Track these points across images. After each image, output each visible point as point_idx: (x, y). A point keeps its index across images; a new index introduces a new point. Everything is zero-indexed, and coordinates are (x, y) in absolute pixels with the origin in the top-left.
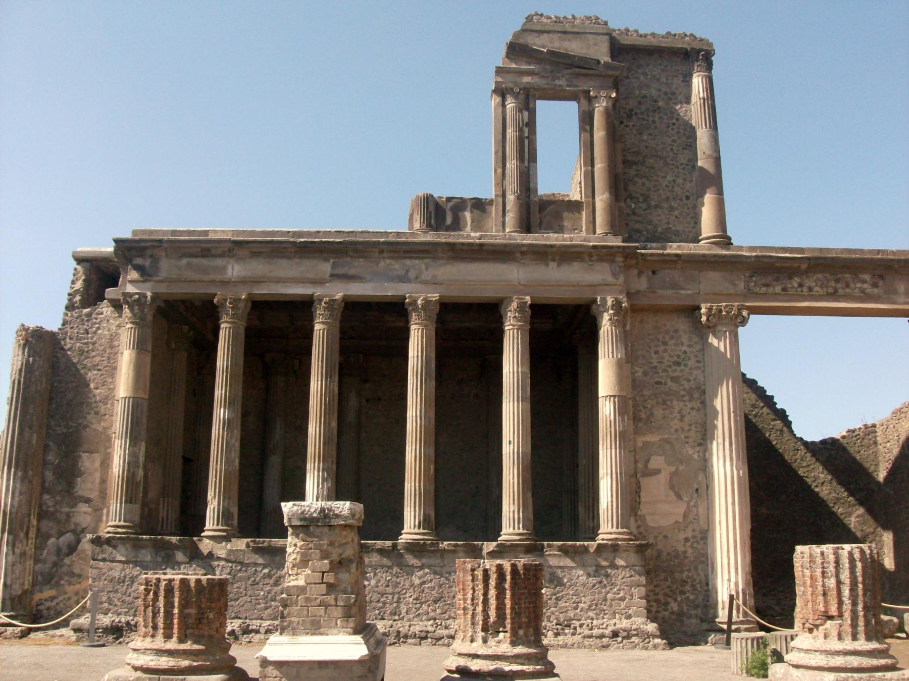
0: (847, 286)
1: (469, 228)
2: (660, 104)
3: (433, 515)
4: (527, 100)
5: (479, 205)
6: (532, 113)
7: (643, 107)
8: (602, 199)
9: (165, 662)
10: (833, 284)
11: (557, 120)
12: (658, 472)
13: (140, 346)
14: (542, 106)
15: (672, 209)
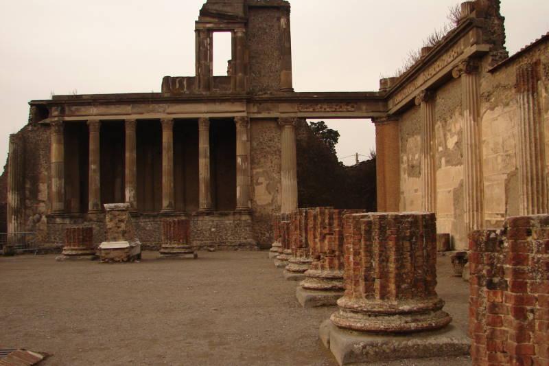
0: (341, 107)
1: (185, 90)
2: (267, 31)
3: (173, 202)
5: (189, 79)
6: (211, 39)
7: (260, 32)
9: (74, 253)
10: (334, 107)
12: (262, 183)
13: (59, 142)
14: (216, 35)
15: (270, 76)
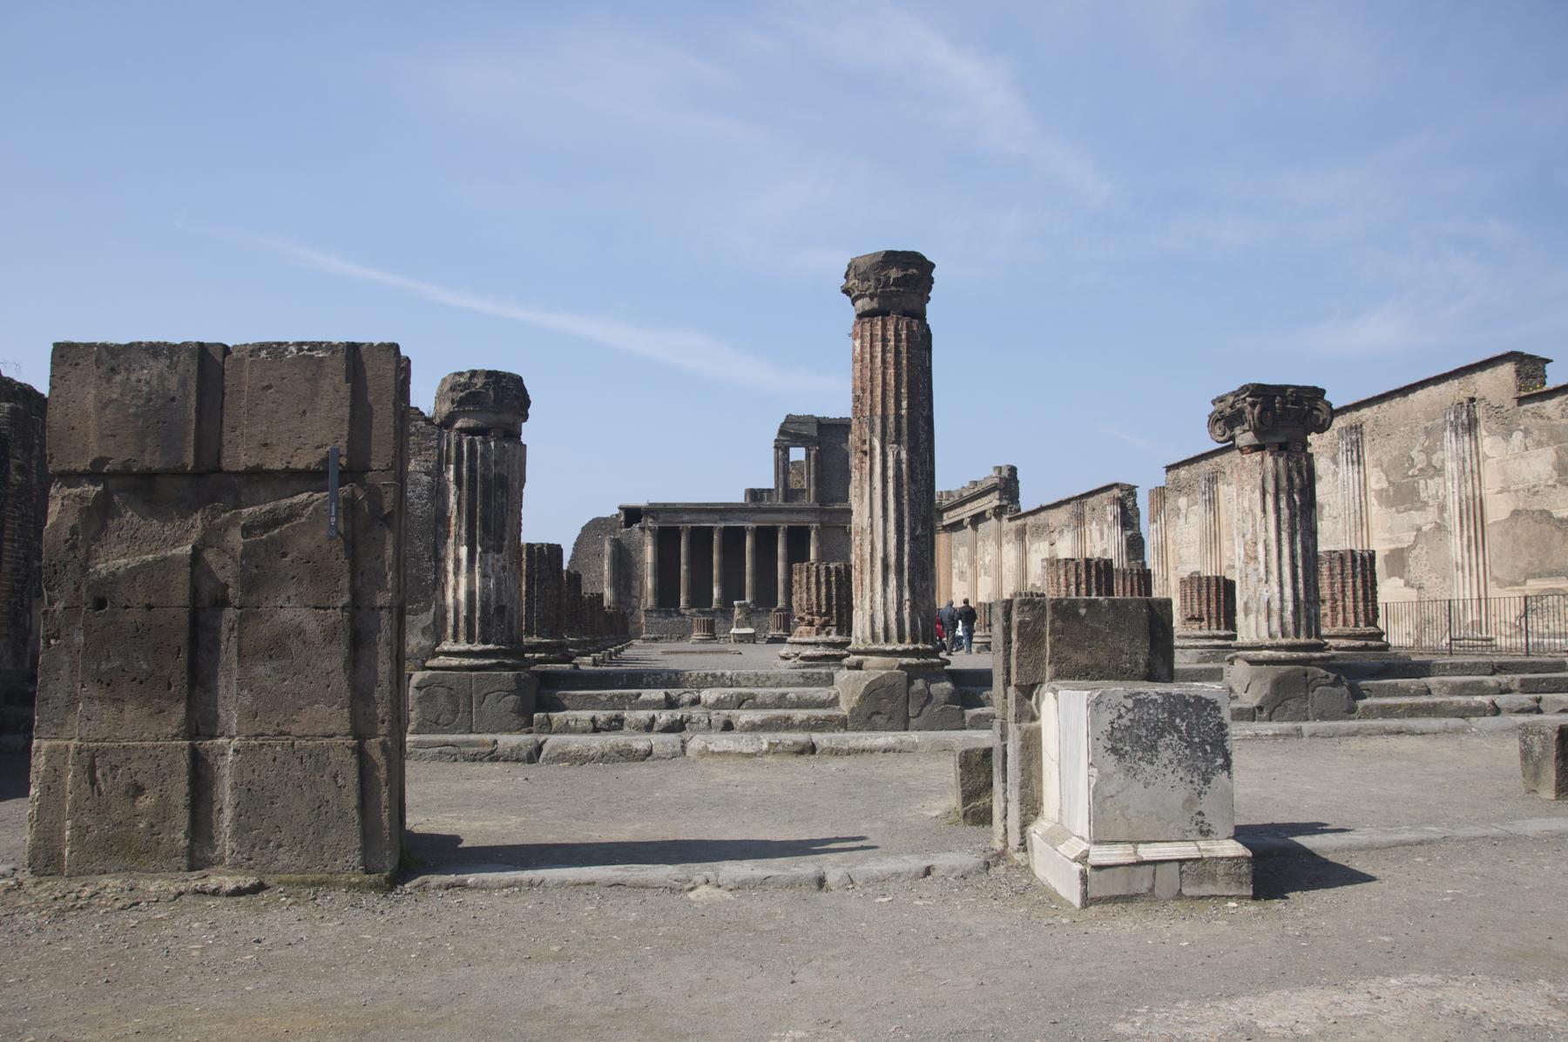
4: (786, 452)
8: (812, 489)
11: (798, 454)
